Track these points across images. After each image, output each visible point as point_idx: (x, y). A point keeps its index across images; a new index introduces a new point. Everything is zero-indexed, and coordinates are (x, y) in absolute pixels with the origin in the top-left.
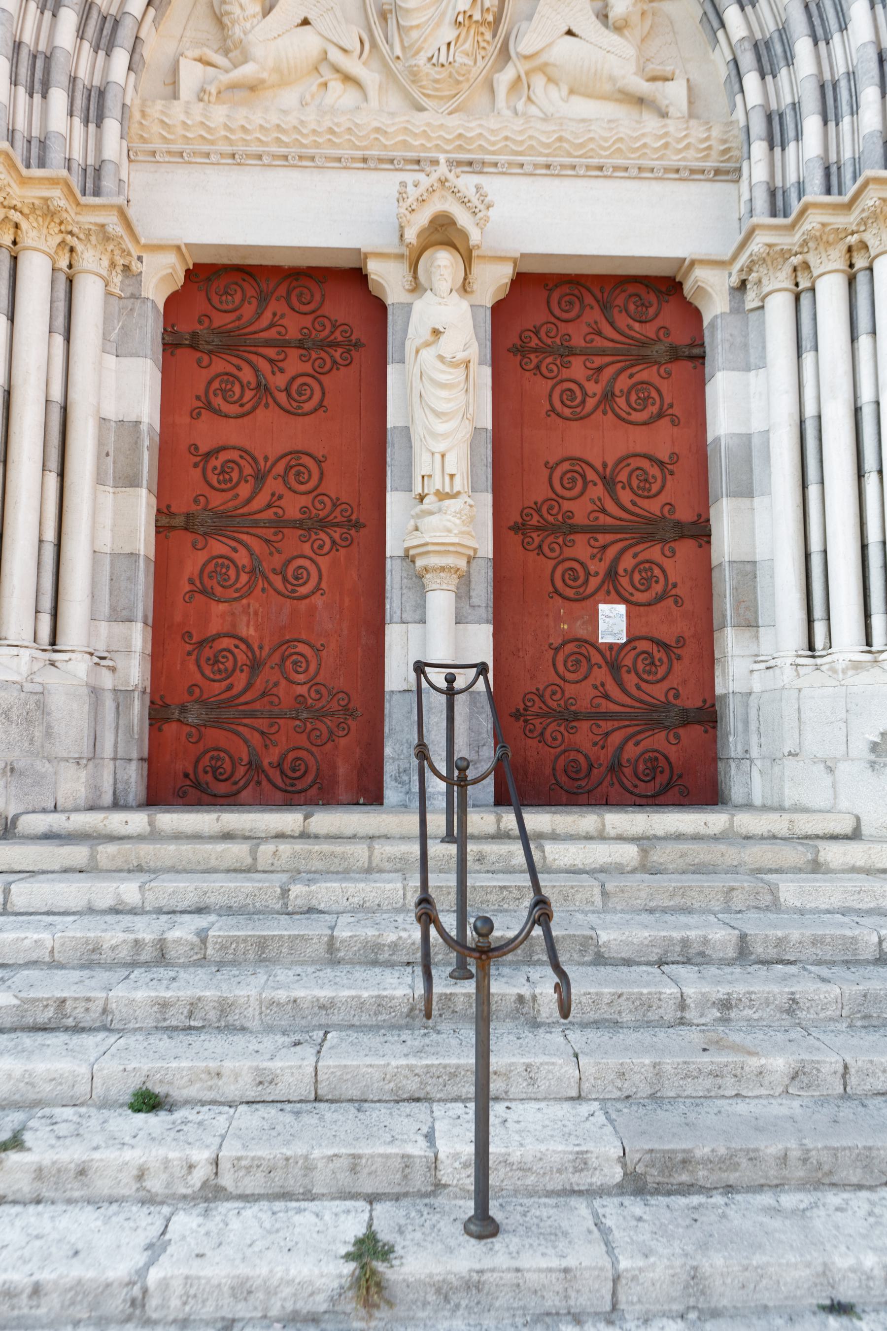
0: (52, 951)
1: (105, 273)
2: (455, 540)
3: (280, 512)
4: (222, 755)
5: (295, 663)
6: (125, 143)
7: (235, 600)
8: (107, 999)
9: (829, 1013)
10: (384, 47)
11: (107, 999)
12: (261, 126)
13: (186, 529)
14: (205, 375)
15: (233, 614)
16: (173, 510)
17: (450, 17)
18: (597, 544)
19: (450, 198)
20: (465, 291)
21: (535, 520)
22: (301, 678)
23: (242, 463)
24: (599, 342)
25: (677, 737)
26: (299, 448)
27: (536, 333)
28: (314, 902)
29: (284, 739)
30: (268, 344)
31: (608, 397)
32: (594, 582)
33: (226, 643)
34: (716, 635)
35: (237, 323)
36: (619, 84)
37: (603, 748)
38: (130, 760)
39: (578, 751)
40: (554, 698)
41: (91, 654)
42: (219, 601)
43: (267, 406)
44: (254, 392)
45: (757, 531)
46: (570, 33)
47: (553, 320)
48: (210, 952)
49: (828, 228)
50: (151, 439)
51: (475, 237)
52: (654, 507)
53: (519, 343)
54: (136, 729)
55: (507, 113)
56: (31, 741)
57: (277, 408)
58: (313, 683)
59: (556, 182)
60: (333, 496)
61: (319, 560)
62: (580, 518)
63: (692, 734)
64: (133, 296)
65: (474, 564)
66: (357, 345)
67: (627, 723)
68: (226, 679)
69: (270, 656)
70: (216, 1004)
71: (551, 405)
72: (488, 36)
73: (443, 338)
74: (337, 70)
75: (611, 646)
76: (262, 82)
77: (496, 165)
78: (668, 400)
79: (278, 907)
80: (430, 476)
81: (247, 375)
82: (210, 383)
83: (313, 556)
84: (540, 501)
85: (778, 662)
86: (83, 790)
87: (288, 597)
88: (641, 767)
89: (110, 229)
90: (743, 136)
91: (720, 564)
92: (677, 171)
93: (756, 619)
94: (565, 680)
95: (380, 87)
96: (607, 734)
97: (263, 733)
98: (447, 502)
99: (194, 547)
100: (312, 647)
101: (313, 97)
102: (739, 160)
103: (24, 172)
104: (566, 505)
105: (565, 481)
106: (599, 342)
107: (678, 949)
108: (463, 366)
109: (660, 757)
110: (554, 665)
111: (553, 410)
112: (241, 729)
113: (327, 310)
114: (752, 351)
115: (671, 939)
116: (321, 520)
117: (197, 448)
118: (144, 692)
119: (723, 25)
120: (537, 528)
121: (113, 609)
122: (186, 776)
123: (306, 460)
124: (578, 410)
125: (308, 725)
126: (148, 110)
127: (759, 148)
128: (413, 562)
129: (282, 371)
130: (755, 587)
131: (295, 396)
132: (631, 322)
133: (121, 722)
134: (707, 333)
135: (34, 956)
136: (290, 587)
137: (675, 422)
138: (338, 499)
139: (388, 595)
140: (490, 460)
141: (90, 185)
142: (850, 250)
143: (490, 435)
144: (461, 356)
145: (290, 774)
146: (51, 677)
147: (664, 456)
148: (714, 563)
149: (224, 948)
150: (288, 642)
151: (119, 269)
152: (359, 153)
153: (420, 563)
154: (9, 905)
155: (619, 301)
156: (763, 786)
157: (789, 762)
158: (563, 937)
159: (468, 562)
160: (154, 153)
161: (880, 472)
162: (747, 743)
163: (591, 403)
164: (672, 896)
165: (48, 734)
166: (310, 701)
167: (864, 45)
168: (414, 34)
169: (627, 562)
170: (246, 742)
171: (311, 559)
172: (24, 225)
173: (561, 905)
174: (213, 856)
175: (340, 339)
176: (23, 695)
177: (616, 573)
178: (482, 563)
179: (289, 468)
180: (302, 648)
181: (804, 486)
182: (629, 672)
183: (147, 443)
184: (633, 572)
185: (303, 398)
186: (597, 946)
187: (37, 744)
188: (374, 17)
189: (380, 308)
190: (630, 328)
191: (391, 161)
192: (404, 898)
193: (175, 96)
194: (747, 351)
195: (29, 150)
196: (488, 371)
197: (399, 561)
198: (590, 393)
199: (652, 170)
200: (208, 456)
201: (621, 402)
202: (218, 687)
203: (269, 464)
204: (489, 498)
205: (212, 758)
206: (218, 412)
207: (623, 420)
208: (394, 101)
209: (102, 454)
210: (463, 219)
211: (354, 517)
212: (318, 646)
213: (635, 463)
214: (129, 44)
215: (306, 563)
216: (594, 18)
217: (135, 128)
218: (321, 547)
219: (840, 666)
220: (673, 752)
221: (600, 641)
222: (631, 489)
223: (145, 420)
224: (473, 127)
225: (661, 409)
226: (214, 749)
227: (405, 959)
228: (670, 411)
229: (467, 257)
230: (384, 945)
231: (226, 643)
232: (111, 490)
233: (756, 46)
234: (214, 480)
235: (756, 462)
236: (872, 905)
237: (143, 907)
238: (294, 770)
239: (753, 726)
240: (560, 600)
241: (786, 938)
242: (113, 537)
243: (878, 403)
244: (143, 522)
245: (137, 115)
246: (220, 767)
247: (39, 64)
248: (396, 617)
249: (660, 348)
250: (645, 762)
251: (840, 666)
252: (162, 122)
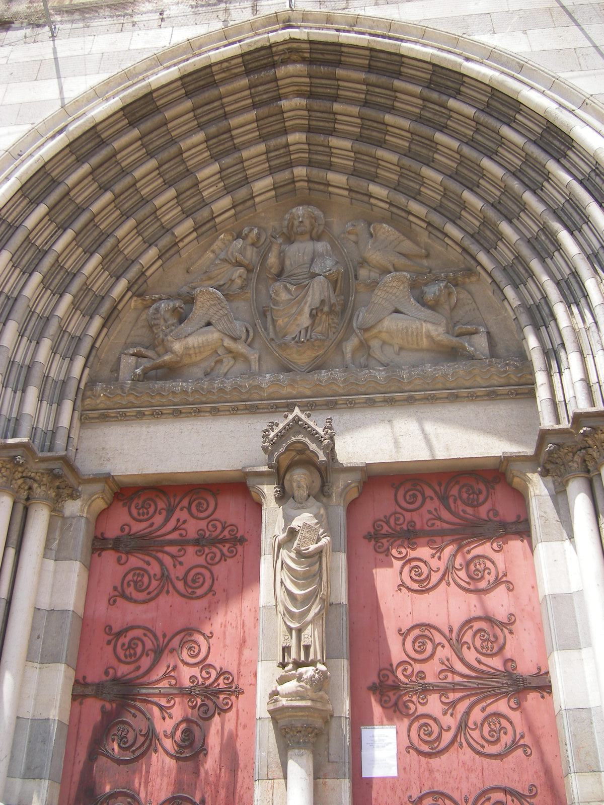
14: (121, 570)
30: (172, 543)
35: (150, 529)
46: (397, 311)
81: (155, 569)
93: (598, 767)
117: (111, 628)
121: (28, 768)
129: (181, 563)
131: (191, 584)
155: (455, 491)
163: (435, 578)
175: (228, 536)
177: (466, 725)
185: (197, 585)
190: (464, 512)
200: (119, 634)
232: (38, 666)
242: (35, 705)
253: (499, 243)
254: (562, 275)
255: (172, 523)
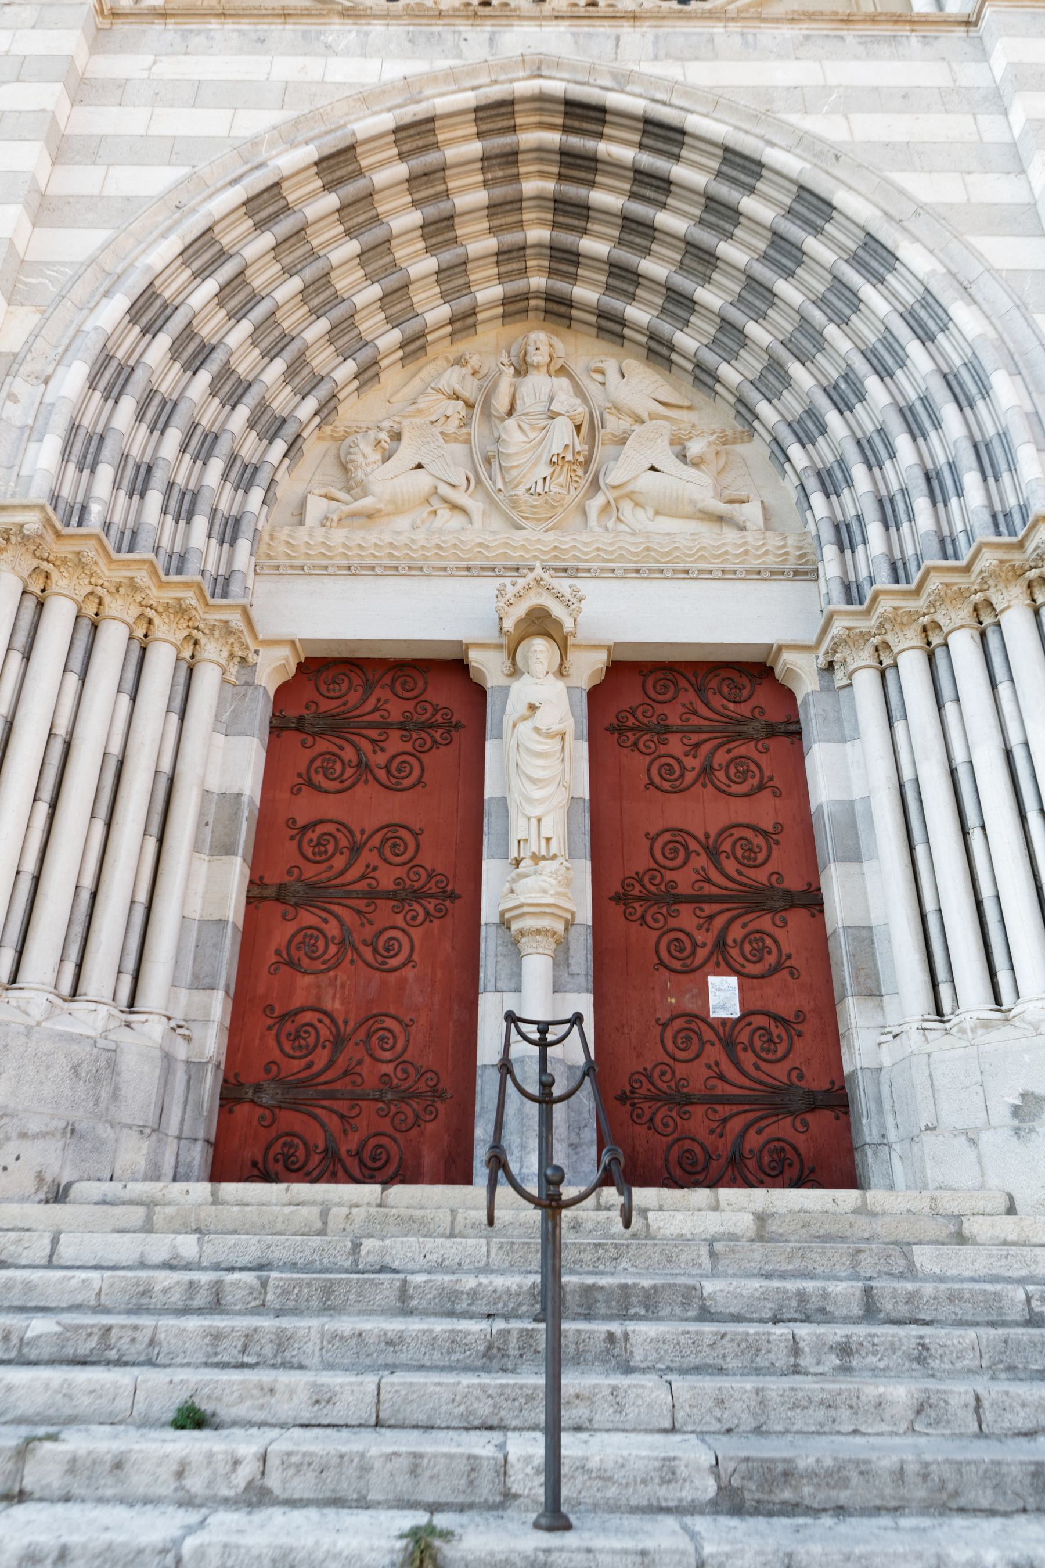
0: (99, 1294)
1: (224, 663)
2: (551, 901)
3: (374, 883)
4: (296, 1141)
5: (382, 1039)
6: (253, 559)
7: (322, 972)
8: (156, 1327)
9: (966, 1362)
10: (488, 484)
11: (156, 1327)
12: (376, 544)
13: (277, 900)
14: (309, 754)
15: (319, 987)
16: (265, 881)
17: (546, 458)
18: (703, 914)
19: (545, 594)
20: (562, 675)
21: (637, 891)
22: (387, 1055)
23: (339, 835)
24: (695, 721)
25: (805, 1124)
26: (396, 821)
27: (633, 713)
28: (388, 1259)
29: (365, 1123)
30: (371, 726)
31: (707, 771)
32: (702, 954)
33: (309, 1017)
34: (838, 1008)
36: (700, 506)
37: (721, 1136)
38: (196, 1140)
39: (693, 1140)
40: (664, 1078)
41: (169, 1019)
42: (305, 973)
43: (366, 782)
44: (353, 770)
45: (869, 896)
46: (653, 469)
47: (648, 701)
48: (270, 1297)
49: (900, 612)
50: (251, 811)
51: (568, 625)
52: (761, 876)
53: (616, 722)
54: (205, 1105)
55: (600, 530)
56: (97, 1102)
57: (376, 784)
58: (399, 1061)
59: (646, 583)
60: (429, 867)
61: (412, 931)
62: (684, 888)
63: (821, 1121)
64: (247, 684)
65: (572, 931)
66: (457, 726)
67: (747, 1107)
68: (306, 1056)
69: (355, 1031)
70: (273, 1337)
71: (650, 778)
72: (580, 472)
73: (539, 712)
74: (446, 501)
75: (724, 1022)
76: (379, 511)
77: (589, 570)
78: (767, 773)
79: (347, 1264)
80: (526, 840)
82: (312, 761)
83: (406, 927)
84: (641, 871)
85: (904, 1028)
86: (143, 1163)
87: (377, 969)
88: (766, 1159)
89: (232, 624)
90: (816, 543)
91: (835, 931)
92: (759, 573)
93: (879, 989)
94: (675, 1059)
95: (484, 513)
96: (725, 1121)
97: (342, 1117)
98: (542, 863)
99: (284, 918)
100: (400, 1022)
101: (423, 522)
102: (815, 563)
103: (164, 578)
104: (669, 875)
105: (667, 852)
106: (695, 721)
107: (794, 1303)
108: (559, 738)
109: (788, 1148)
110: (662, 1042)
111: (652, 783)
112: (318, 1111)
113: (428, 696)
114: (845, 724)
115: (785, 1291)
116: (415, 891)
118: (218, 1067)
119: (789, 460)
120: (639, 899)
121: (195, 976)
122: (255, 1164)
123: (402, 833)
124: (677, 783)
125: (392, 1107)
126: (276, 534)
127: (830, 551)
128: (509, 928)
129: (383, 750)
130: (873, 954)
132: (725, 702)
133: (190, 1097)
134: (801, 711)
135: (79, 1299)
136: (380, 959)
137: (777, 793)
138: (433, 870)
139: (482, 963)
140: (588, 828)
141: (219, 590)
142: (925, 629)
143: (587, 804)
144: (556, 727)
145: (370, 1164)
146: (125, 1037)
147: (767, 825)
148: (829, 931)
149: (285, 1293)
150: (376, 1016)
151: (237, 660)
152: (464, 564)
153: (515, 926)
154: (55, 1257)
155: (714, 684)
156: (906, 1174)
157: (928, 1138)
158: (663, 1286)
159: (566, 929)
160: (278, 567)
161: (983, 827)
162: (882, 1126)
163: (689, 777)
164: (790, 1258)
165: (115, 1096)
166: (395, 1081)
167: (910, 467)
168: (514, 472)
169: (736, 932)
170: (323, 1126)
171: (403, 930)
172: (157, 621)
173: (665, 1267)
174: (280, 1219)
175: (441, 720)
176: (95, 1051)
177: (725, 944)
178: (582, 929)
179: (385, 840)
180: (389, 1023)
181: (911, 848)
182: (745, 1050)
183: (246, 814)
184: (743, 942)
185: (403, 774)
186: (702, 1298)
187: (102, 1106)
188: (479, 461)
189: (480, 693)
191: (493, 569)
192: (488, 1256)
193: (301, 523)
194: (841, 725)
195: (170, 563)
196: (584, 746)
197: (494, 928)
198: (689, 767)
199: (735, 572)
200: (304, 829)
201: (721, 775)
202: (297, 1065)
203: (365, 836)
204: (587, 865)
205: (285, 1144)
206: (318, 788)
207: (723, 792)
208: (496, 523)
209: (202, 823)
210: (557, 610)
211: (449, 888)
212: (407, 1021)
213: (738, 833)
214: (265, 483)
215: (398, 934)
216: (673, 457)
217: (263, 548)
218: (414, 918)
219: (967, 1025)
220: (801, 1141)
221: (712, 1015)
222: (736, 858)
223: (247, 792)
224: (567, 541)
225: (761, 781)
226: (288, 1135)
227: (485, 1310)
228: (770, 784)
229: (563, 645)
230: (462, 1292)
231: (309, 1017)
232: (207, 858)
233: (819, 474)
234: (309, 852)
235: (861, 827)
236: (1024, 1273)
237: (199, 1262)
238: (374, 1159)
239: (887, 1106)
240: (666, 973)
241: (917, 1292)
243: (971, 762)
244: (235, 889)
245: (266, 538)
246: (293, 1155)
247: (188, 498)
248: (490, 986)
249: (757, 725)
250: (771, 1153)
251: (967, 1025)
252: (288, 543)
253: (785, 393)
254: (863, 432)
255: (372, 702)
